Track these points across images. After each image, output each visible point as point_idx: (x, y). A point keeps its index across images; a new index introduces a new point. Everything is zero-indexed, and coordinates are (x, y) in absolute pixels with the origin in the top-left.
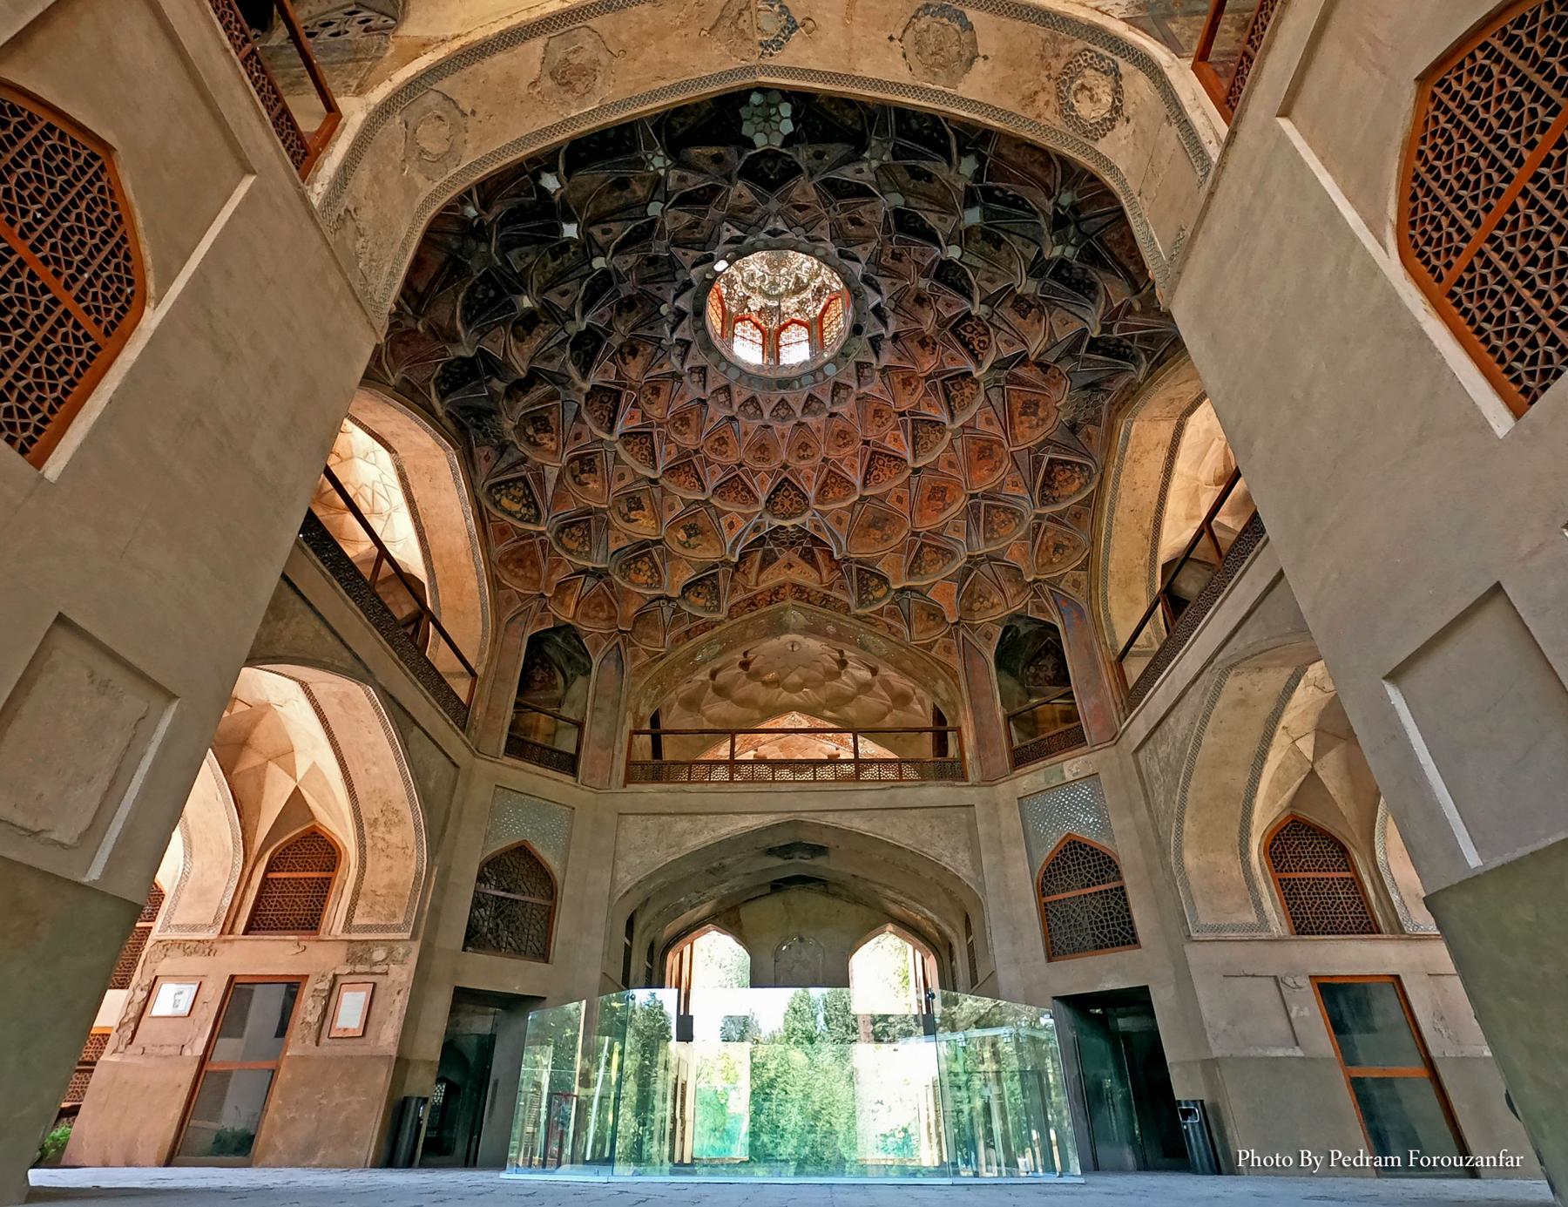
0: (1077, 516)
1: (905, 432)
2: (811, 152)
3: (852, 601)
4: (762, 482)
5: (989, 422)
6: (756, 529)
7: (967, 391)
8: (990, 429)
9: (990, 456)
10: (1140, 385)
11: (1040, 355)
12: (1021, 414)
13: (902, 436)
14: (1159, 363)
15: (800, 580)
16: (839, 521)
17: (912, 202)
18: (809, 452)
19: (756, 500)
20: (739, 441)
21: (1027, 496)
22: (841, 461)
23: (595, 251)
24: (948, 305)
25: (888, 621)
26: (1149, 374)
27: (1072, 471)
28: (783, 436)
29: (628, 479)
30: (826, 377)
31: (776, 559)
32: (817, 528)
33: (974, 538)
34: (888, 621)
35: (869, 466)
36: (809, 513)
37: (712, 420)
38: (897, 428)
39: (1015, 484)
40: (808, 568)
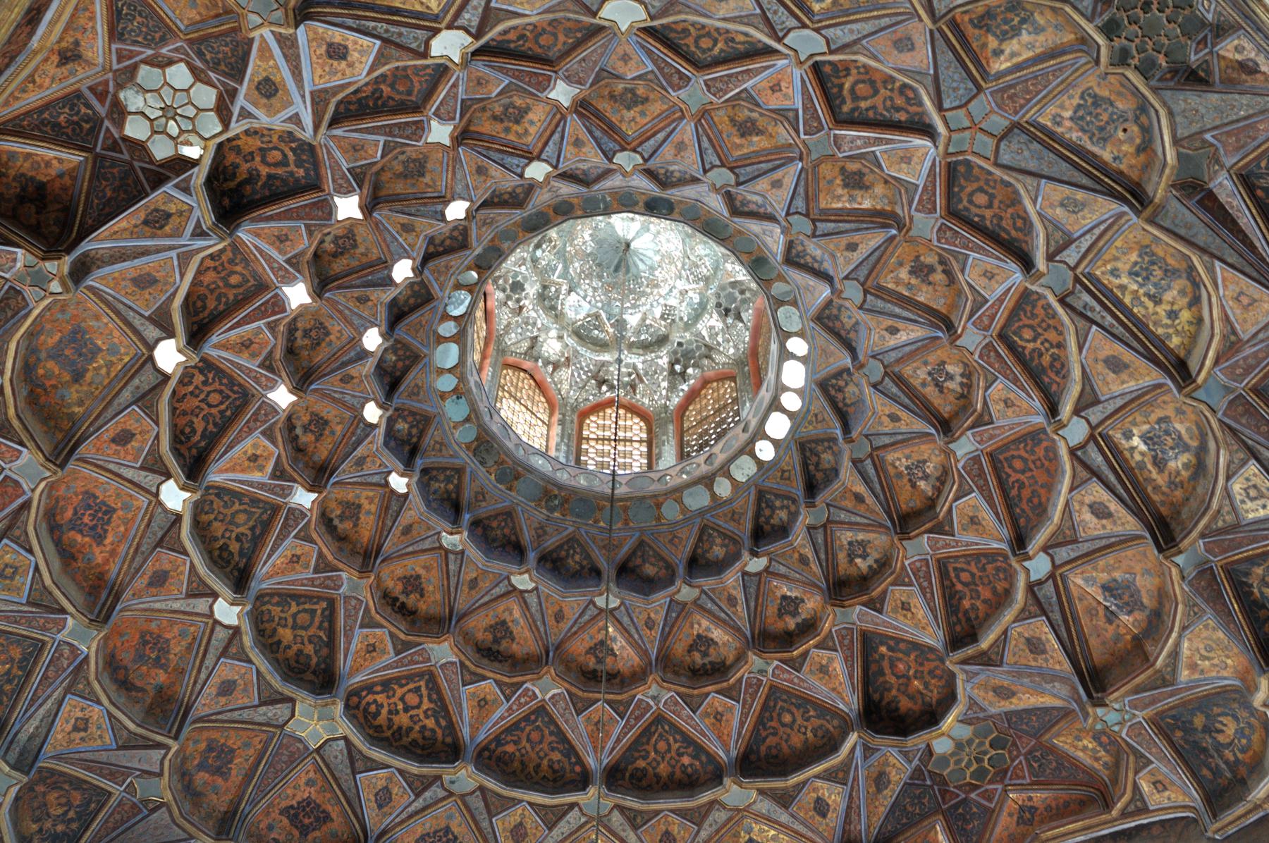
1: (262, 486)
2: (894, 776)
5: (227, 688)
8: (210, 690)
13: (257, 476)
22: (272, 327)
23: (1096, 458)
27: (62, 818)
30: (441, 340)
36: (208, 219)
38: (279, 473)
39: (82, 725)
40: (33, 98)
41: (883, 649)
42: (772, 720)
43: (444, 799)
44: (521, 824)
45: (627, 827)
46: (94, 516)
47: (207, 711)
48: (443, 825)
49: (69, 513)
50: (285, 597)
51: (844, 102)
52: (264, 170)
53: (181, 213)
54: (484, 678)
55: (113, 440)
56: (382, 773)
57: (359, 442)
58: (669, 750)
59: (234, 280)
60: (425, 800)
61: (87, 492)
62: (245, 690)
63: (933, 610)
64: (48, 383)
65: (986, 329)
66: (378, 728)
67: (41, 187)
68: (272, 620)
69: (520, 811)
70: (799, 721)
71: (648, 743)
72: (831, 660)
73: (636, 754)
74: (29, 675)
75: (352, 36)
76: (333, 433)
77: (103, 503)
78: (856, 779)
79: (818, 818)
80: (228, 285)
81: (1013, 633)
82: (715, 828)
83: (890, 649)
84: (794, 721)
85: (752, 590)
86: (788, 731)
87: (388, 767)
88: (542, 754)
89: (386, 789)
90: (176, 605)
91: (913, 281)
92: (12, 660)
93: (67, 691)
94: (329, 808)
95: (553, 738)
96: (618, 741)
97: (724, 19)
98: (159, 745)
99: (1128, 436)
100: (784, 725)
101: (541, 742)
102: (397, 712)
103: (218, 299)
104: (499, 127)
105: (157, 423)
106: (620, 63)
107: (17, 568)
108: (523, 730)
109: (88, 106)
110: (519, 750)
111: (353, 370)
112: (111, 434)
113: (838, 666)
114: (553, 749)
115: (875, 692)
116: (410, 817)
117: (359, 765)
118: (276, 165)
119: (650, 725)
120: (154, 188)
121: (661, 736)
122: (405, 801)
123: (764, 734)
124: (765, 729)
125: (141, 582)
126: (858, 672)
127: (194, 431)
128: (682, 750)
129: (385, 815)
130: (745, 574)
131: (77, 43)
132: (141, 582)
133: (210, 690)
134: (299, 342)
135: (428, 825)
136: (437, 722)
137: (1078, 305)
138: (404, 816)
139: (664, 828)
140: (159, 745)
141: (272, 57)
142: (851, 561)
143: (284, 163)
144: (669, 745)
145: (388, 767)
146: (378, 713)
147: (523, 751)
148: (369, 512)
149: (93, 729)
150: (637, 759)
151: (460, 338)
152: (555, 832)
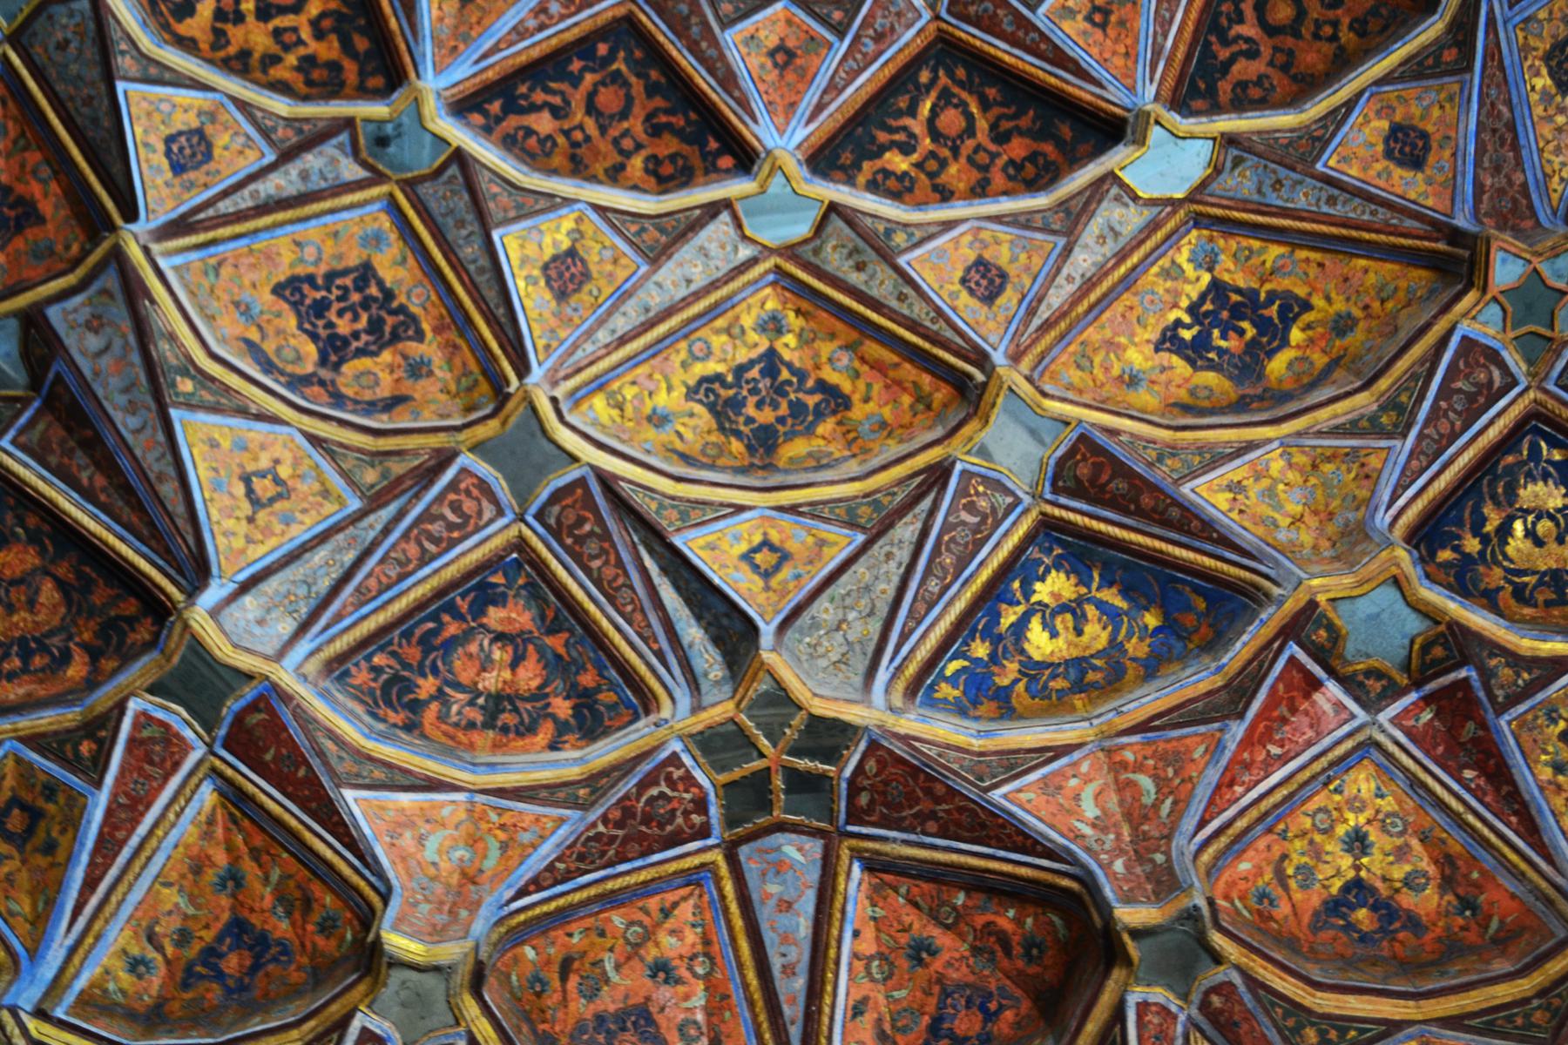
11: (133, 291)
17: (1131, 219)
42: (1241, 21)
43: (359, 185)
44: (572, 253)
45: (871, 255)
48: (353, 260)
58: (970, 130)
60: (304, 175)
69: (568, 225)
71: (912, 111)
73: (883, 137)
78: (1493, 52)
79: (1398, 172)
82: (1110, 248)
86: (1289, 41)
88: (627, 144)
94: (36, 189)
95: (658, 102)
96: (833, 88)
101: (624, 115)
102: (239, 18)
108: (576, 81)
110: (567, 133)
114: (656, 131)
116: (262, 209)
117: (125, 63)
121: (945, 95)
122: (250, 162)
123: (1224, 54)
124: (1226, 42)
128: (1006, 125)
129: (189, 186)
135: (310, 253)
136: (347, 46)
138: (243, 200)
139: (972, 256)
144: (970, 118)
147: (578, 136)
150: (883, 149)
152: (669, 273)
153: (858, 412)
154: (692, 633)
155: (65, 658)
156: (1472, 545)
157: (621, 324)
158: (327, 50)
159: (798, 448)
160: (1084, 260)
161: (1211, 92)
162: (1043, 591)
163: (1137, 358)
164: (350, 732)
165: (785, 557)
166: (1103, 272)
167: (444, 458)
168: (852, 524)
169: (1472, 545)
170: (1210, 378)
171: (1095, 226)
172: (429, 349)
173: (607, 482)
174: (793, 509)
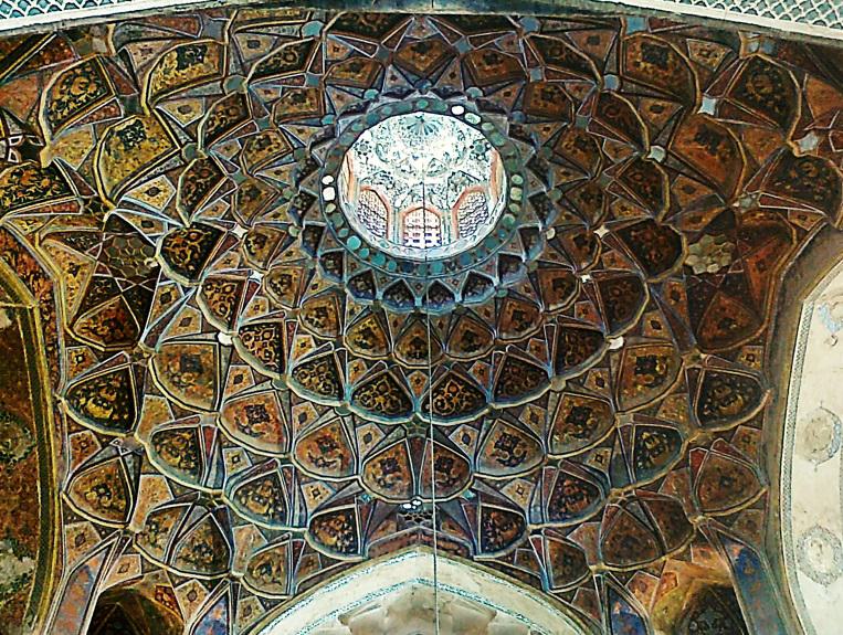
0: (308, 563)
1: (317, 352)
3: (66, 384)
4: (215, 209)
5: (367, 438)
6: (148, 224)
7: (380, 399)
9: (324, 450)
10: (472, 559)
12: (380, 461)
13: (311, 351)
14: (503, 569)
15: (61, 297)
16: (186, 322)
17: (616, 356)
18: (254, 248)
19: (190, 210)
20: (271, 165)
21: (310, 511)
22: (260, 293)
24: (481, 372)
25: (69, 446)
26: (486, 563)
28: (276, 216)
29: (247, 53)
30: (344, 240)
31: (82, 249)
32: (166, 298)
33: (232, 482)
34: (69, 446)
35: (257, 325)
36: (186, 282)
37: (300, 132)
39: (316, 493)
40: (79, 295)
41: (633, 233)
46: (257, 413)
47: (366, 453)
49: (247, 419)
50: (367, 386)
51: (371, 28)
52: (195, 243)
53: (172, 289)
54: (474, 362)
55: (235, 383)
56: (459, 430)
57: (344, 306)
59: (228, 289)
61: (245, 408)
62: (376, 435)
63: (636, 203)
64: (191, 382)
65: (537, 65)
66: (448, 410)
67: (114, 320)
68: (369, 398)
70: (623, 290)
72: (613, 254)
74: (281, 488)
75: (151, 182)
76: (331, 310)
77: (256, 406)
80: (228, 293)
81: (675, 191)
83: (636, 231)
84: (621, 292)
85: (558, 246)
87: (459, 425)
89: (465, 435)
90: (320, 422)
91: (494, 66)
92: (270, 487)
93: (299, 484)
96: (550, 350)
97: (271, 51)
98: (352, 481)
99: (638, 64)
100: (618, 296)
103: (229, 301)
104: (265, 151)
105: (247, 364)
106: (268, 96)
107: (238, 456)
109: (103, 278)
111: (313, 282)
112: (232, 381)
113: (618, 255)
115: (644, 254)
116: (483, 439)
117: (446, 432)
118: (198, 238)
119: (560, 334)
120: (154, 288)
125: (296, 424)
126: (629, 252)
127: (270, 353)
130: (549, 241)
131: (71, 264)
132: (296, 424)
133: (361, 442)
134: (282, 289)
137: (550, 28)
140: (352, 481)
141: (133, 215)
142: (588, 203)
143: (199, 235)
145: (459, 425)
146: (443, 405)
148: (375, 328)
149: (321, 491)
151: (352, 232)
153: (595, 411)
154: (596, 474)
155: (511, 525)
156: (709, 400)
157: (549, 422)
158: (468, 394)
159: (589, 422)
160: (614, 370)
161: (614, 316)
162: (644, 437)
163: (634, 379)
164: (560, 525)
165: (602, 457)
166: (618, 368)
167: (541, 470)
168: (608, 447)
169: (709, 400)
170: (648, 375)
171: (612, 361)
172: (523, 441)
173: (567, 459)
174: (597, 447)
